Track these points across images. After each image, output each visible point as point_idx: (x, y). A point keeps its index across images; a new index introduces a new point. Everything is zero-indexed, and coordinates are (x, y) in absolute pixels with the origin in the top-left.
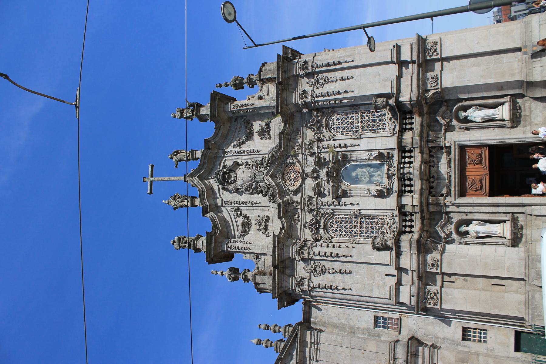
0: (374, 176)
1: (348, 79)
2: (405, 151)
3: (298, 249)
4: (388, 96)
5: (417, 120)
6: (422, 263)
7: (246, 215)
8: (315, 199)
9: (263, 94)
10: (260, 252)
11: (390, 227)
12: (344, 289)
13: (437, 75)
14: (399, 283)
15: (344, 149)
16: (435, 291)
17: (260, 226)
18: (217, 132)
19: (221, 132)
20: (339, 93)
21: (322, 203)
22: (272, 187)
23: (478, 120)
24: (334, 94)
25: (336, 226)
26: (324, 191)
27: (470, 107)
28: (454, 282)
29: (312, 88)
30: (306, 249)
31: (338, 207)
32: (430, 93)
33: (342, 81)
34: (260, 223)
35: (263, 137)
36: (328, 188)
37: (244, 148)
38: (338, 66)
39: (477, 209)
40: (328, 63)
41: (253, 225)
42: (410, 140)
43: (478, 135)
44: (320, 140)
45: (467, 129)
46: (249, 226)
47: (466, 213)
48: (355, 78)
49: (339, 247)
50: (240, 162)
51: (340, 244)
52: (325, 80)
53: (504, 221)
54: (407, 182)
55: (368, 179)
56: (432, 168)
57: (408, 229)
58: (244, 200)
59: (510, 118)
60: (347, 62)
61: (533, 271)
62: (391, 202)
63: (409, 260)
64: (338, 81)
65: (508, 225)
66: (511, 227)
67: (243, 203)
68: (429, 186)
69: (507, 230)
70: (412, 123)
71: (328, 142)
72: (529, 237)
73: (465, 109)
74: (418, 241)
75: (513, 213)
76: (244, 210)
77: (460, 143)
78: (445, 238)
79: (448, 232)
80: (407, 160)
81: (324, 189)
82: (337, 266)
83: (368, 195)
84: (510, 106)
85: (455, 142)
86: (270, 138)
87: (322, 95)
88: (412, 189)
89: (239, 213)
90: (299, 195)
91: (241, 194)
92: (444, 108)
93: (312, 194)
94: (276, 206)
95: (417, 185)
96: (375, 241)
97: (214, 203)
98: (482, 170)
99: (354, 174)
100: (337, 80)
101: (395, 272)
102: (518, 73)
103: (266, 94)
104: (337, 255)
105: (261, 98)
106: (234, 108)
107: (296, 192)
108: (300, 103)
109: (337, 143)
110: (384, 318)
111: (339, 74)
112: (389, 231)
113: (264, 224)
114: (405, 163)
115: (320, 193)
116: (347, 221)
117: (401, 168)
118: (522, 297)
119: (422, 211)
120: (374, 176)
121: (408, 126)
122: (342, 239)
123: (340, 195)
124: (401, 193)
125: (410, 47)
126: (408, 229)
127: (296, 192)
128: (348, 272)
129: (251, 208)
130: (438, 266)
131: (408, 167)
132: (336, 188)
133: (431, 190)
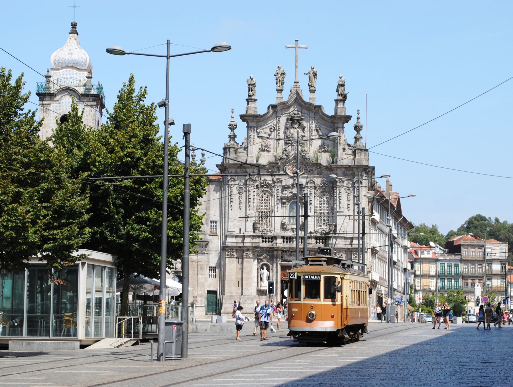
4: (335, 231)
5: (322, 246)
10: (249, 151)
11: (265, 229)
12: (231, 206)
14: (236, 236)
19: (325, 117)
22: (289, 158)
34: (267, 146)
36: (287, 194)
37: (314, 133)
39: (275, 274)
44: (315, 188)
50: (306, 129)
54: (288, 241)
57: (264, 240)
58: (280, 134)
62: (277, 230)
63: (248, 242)
67: (279, 133)
82: (243, 201)
86: (319, 152)
89: (272, 130)
91: (285, 133)
93: (284, 184)
95: (287, 245)
101: (242, 234)
103: (347, 152)
105: (344, 149)
109: (313, 199)
110: (216, 226)
115: (285, 188)
118: (234, 294)
122: (258, 201)
123: (282, 201)
124: (283, 237)
132: (287, 199)
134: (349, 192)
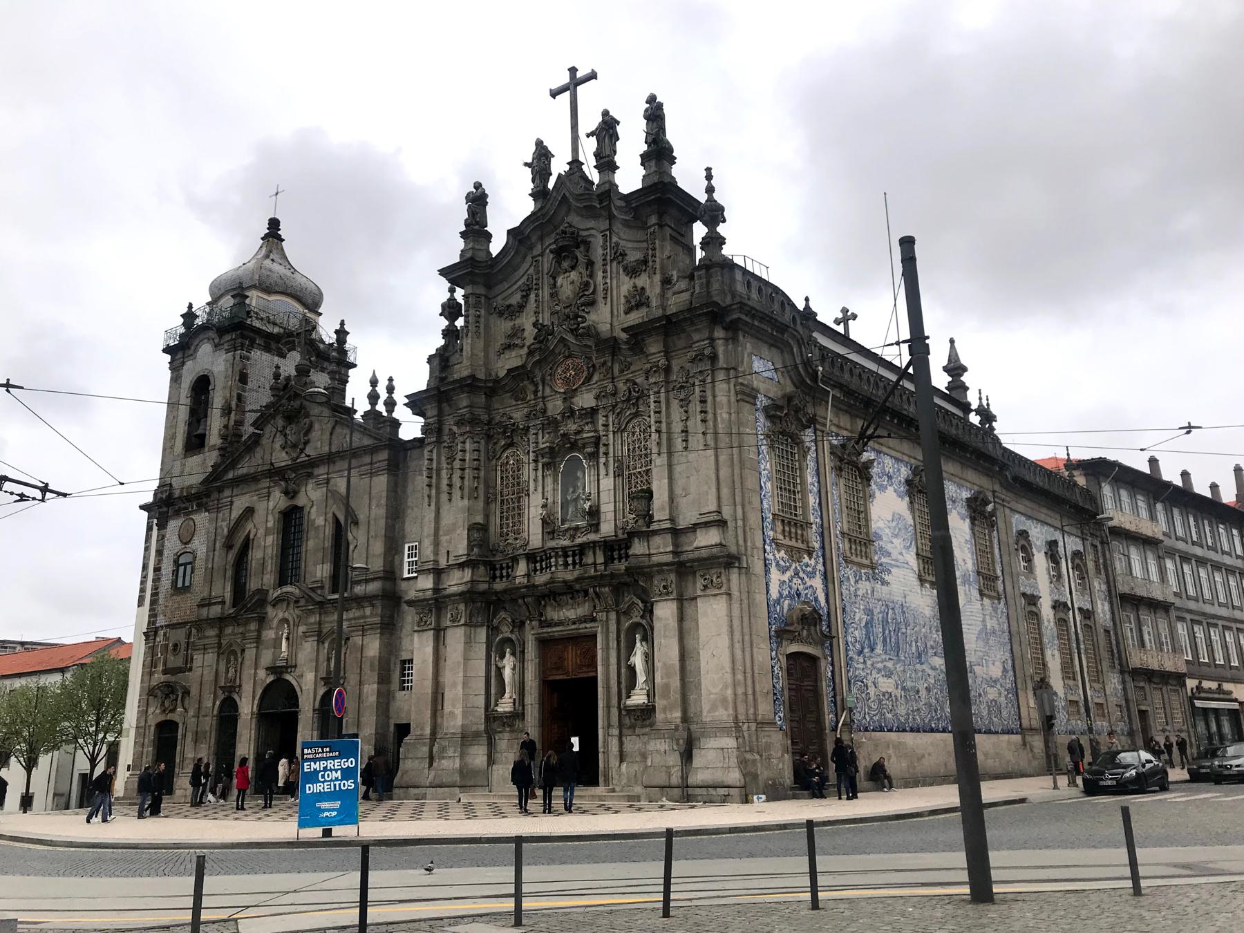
23: (632, 659)
67: (537, 296)
70: (620, 559)
73: (645, 639)
75: (523, 714)
80: (570, 560)
90: (548, 391)
95: (541, 579)
99: (579, 474)
121: (616, 555)
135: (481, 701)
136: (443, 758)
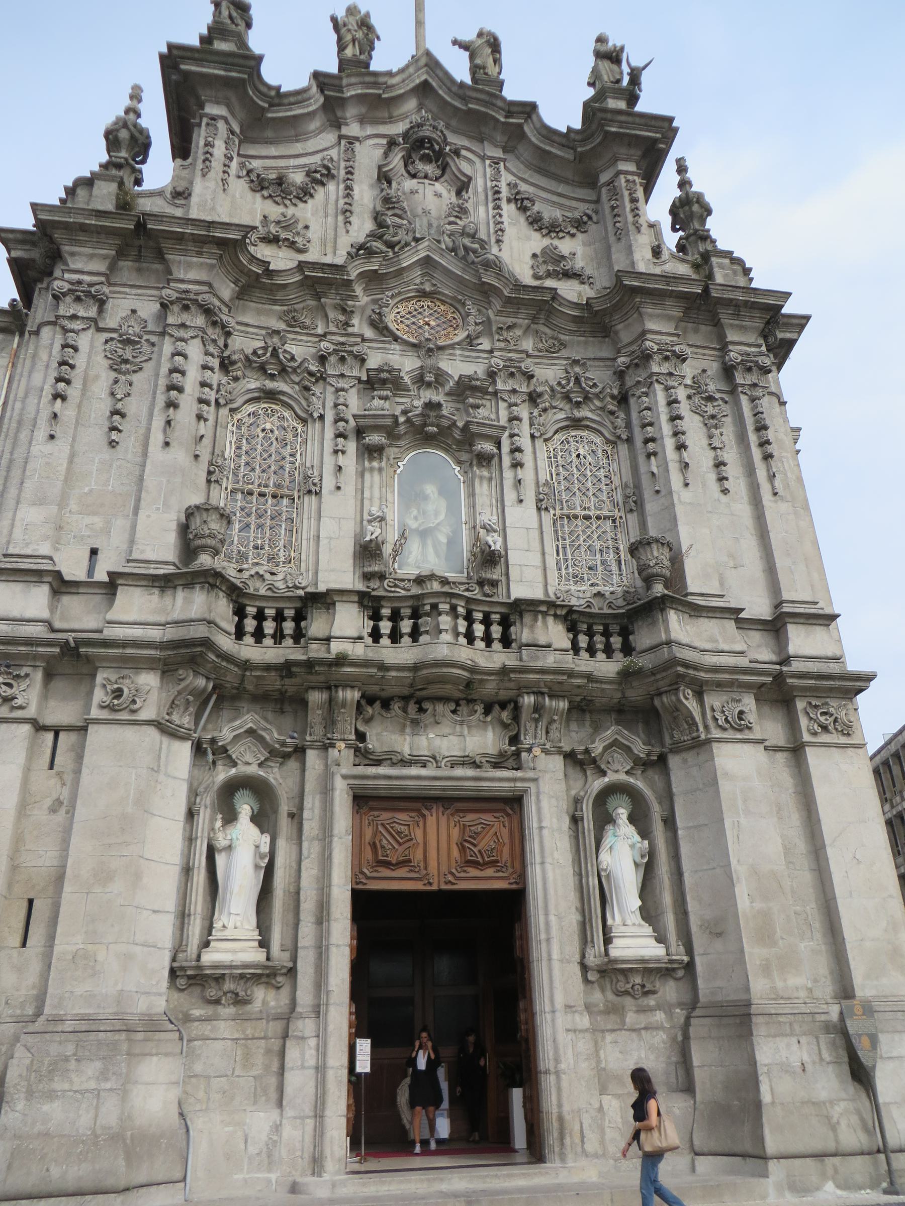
0: (424, 545)
1: (722, 479)
2: (505, 623)
3: (200, 298)
6: (129, 655)
7: (312, 196)
8: (355, 373)
9: (664, 263)
13: (750, 728)
15: (506, 461)
16: (19, 702)
17: (278, 222)
18: (556, 138)
20: (681, 447)
21: (342, 390)
24: (675, 434)
25: (268, 426)
26: (381, 398)
27: (644, 833)
28: (51, 767)
29: (688, 381)
30: (200, 321)
31: (329, 433)
32: (692, 704)
33: (711, 463)
35: (540, 260)
37: (509, 210)
38: (757, 453)
39: (312, 849)
40: (765, 428)
41: (281, 209)
42: (542, 641)
43: (556, 855)
44: (533, 398)
45: (575, 820)
46: (278, 199)
47: (296, 816)
48: (723, 498)
49: (199, 417)
51: (211, 422)
52: (713, 417)
53: (264, 944)
54: (406, 626)
55: (413, 524)
56: (452, 706)
57: (250, 625)
59: (616, 961)
60: (772, 477)
61: (70, 1049)
63: (138, 614)
64: (712, 454)
65: (249, 954)
66: (246, 966)
68: (392, 698)
69: (234, 952)
71: (526, 421)
72: (206, 1029)
73: (639, 820)
74: (207, 643)
75: (292, 972)
76: (327, 195)
77: (533, 798)
78: (213, 741)
79: (234, 752)
80: (479, 630)
81: (386, 398)
83: (366, 517)
84: (658, 961)
85: (535, 780)
87: (672, 402)
88: (385, 641)
89: (320, 176)
90: (369, 333)
92: (640, 748)
94: (339, 260)
96: (215, 516)
97: (348, 115)
98: (444, 869)
99: (430, 489)
100: (715, 448)
102: (774, 989)
104: (172, 405)
106: (627, 181)
107: (378, 325)
108: (648, 343)
109: (525, 442)
111: (731, 455)
112: (246, 574)
113: (283, 236)
114: (469, 618)
116: (284, 458)
117: (454, 608)
119: (310, 664)
120: (424, 545)
125: (830, 654)
126: (250, 625)
127: (378, 325)
128: (114, 435)
129: (331, 210)
130: (112, 708)
131: (455, 627)
133: (378, 704)
134: (710, 409)
135: (164, 930)
136: (51, 1096)
